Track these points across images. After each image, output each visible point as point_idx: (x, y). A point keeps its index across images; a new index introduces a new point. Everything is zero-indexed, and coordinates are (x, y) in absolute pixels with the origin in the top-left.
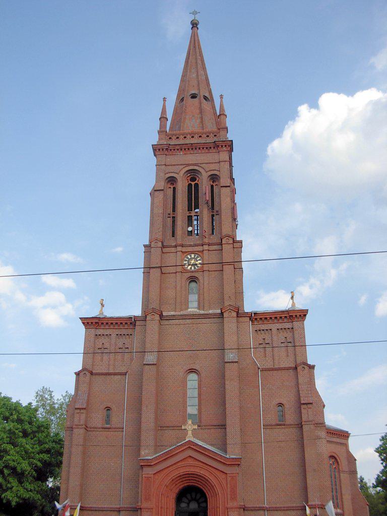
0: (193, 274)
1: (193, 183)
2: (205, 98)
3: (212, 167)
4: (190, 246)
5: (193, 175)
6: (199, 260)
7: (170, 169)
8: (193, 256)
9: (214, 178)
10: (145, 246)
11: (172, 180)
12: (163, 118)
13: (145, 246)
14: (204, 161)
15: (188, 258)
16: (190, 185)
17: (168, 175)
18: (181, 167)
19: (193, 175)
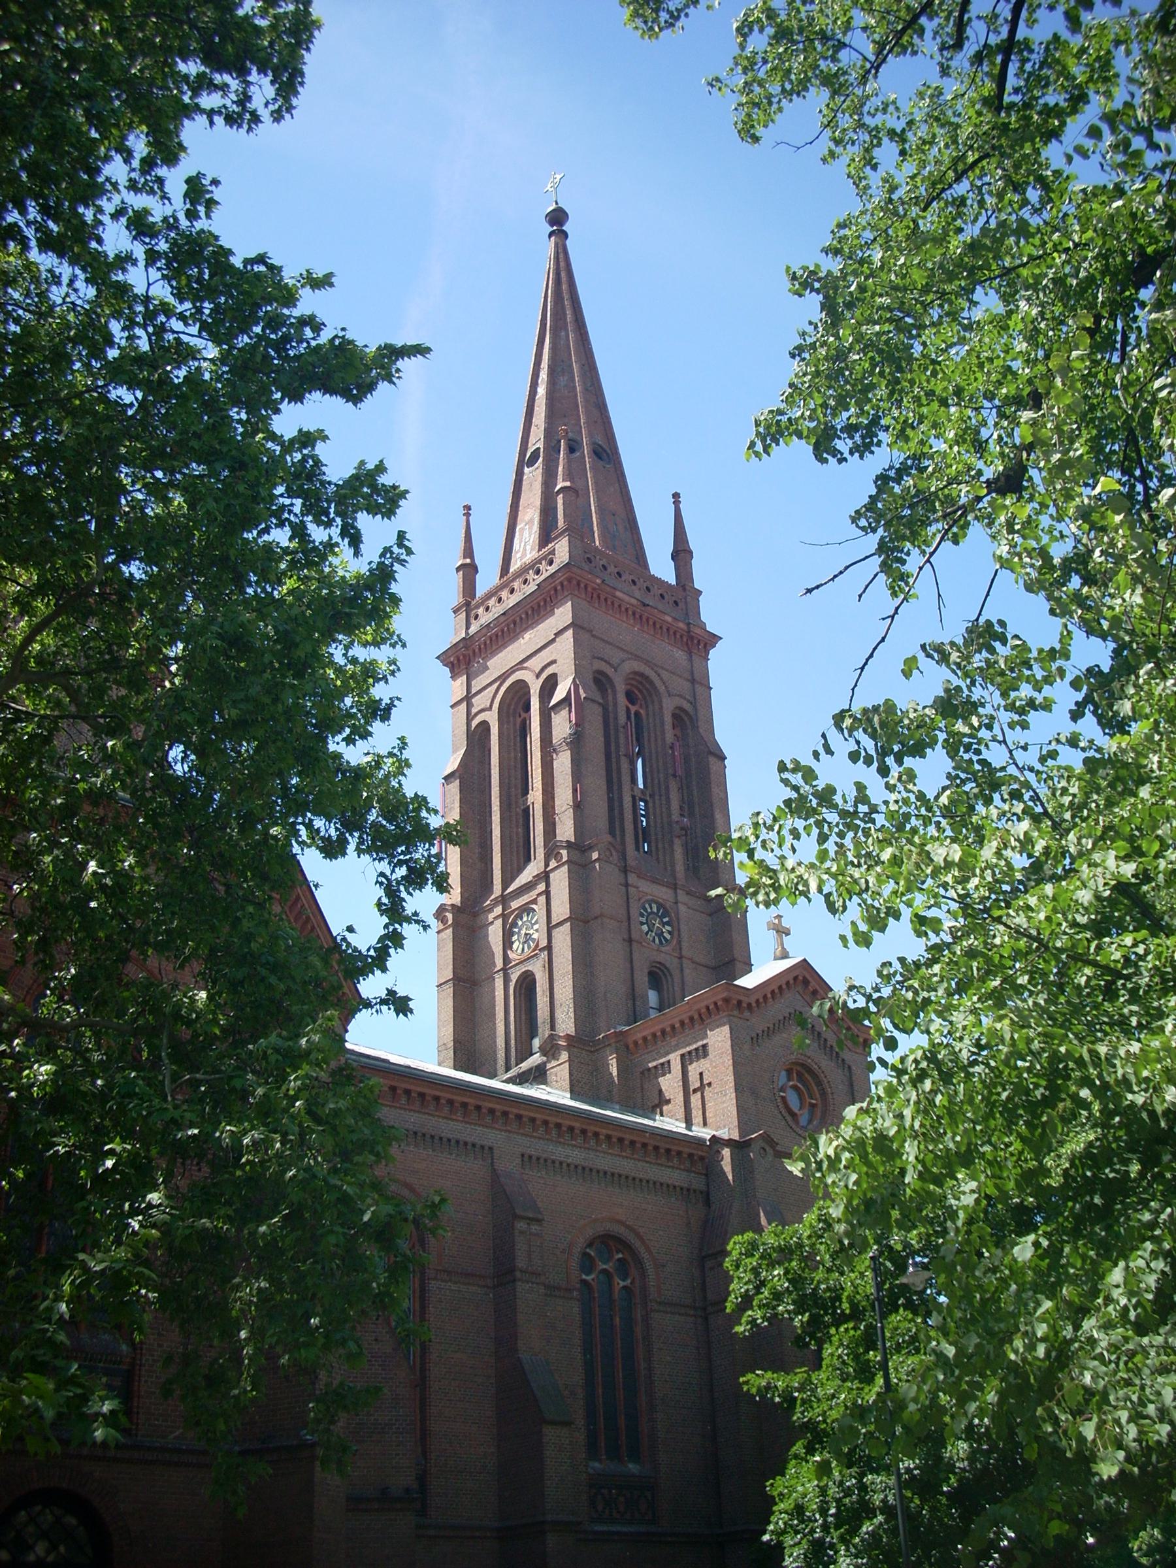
9: (551, 684)
17: (474, 723)
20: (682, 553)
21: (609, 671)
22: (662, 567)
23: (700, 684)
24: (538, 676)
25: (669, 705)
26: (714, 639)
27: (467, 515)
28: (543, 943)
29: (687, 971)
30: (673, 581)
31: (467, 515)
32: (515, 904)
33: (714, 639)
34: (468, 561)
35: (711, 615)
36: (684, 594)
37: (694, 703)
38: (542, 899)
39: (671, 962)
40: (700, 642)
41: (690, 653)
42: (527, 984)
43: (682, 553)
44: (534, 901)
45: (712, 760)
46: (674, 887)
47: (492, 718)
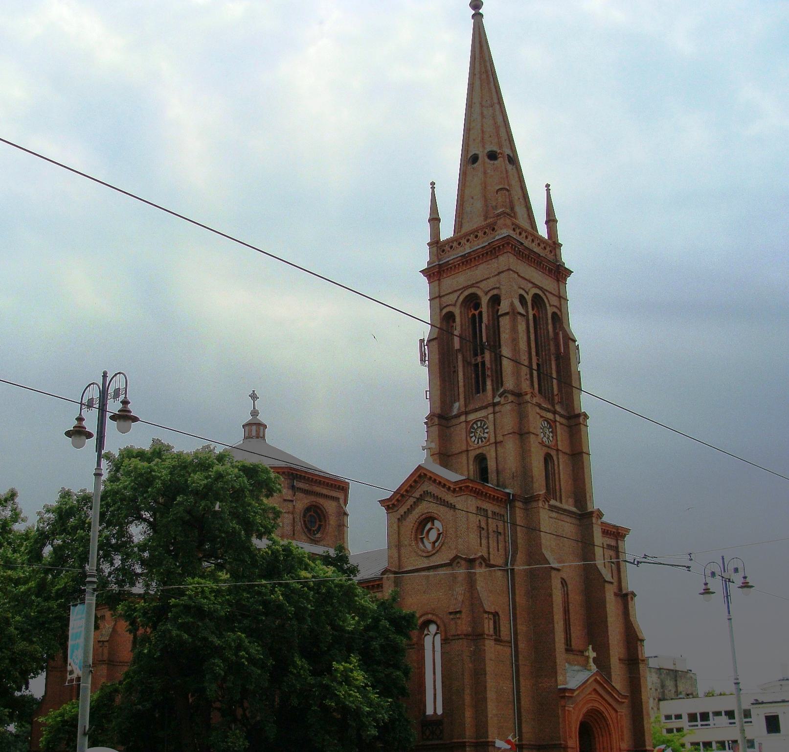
0: (479, 451)
1: (477, 313)
2: (492, 156)
3: (491, 283)
4: (476, 410)
5: (472, 301)
6: (487, 428)
7: (446, 300)
8: (479, 424)
9: (496, 300)
10: (426, 423)
11: (449, 318)
12: (435, 220)
13: (426, 423)
14: (483, 277)
15: (474, 428)
16: (474, 315)
17: (445, 311)
18: (456, 295)
19: (472, 301)
20: (551, 221)
21: (525, 295)
22: (543, 231)
23: (562, 298)
24: (486, 293)
25: (550, 310)
26: (569, 272)
27: (433, 188)
28: (492, 440)
29: (560, 456)
30: (546, 237)
31: (433, 188)
32: (472, 417)
33: (569, 272)
34: (435, 216)
35: (568, 257)
36: (554, 245)
37: (560, 311)
38: (491, 417)
39: (553, 453)
40: (560, 273)
41: (558, 281)
42: (481, 459)
43: (551, 221)
44: (487, 417)
45: (571, 343)
46: (555, 412)
47: (457, 311)
